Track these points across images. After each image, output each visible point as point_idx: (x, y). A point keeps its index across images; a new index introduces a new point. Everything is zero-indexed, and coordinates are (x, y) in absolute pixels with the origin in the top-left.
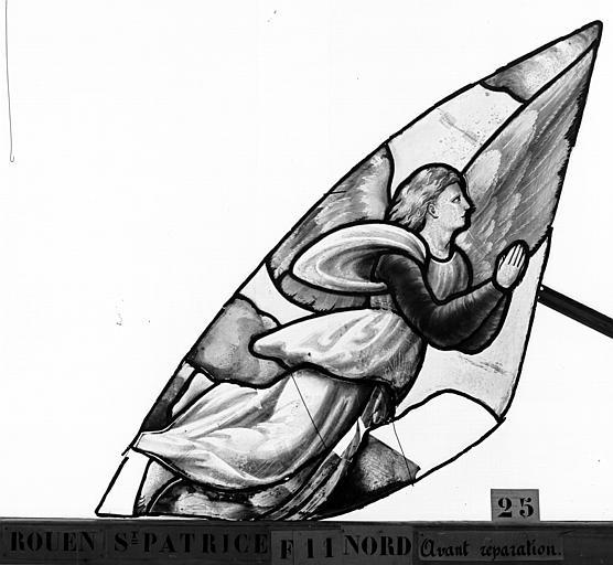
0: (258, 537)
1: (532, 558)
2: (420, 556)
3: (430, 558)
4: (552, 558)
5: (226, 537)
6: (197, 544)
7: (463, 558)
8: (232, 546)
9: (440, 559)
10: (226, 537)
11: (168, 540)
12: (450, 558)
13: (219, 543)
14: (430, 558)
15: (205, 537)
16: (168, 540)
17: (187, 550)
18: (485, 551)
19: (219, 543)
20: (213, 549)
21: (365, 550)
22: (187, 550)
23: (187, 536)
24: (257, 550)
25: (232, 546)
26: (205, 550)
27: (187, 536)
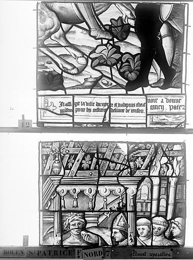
0: (69, 251)
1: (164, 257)
2: (133, 257)
3: (135, 257)
4: (169, 257)
5: (61, 251)
6: (52, 253)
7: (144, 257)
8: (62, 253)
9: (137, 257)
10: (61, 251)
11: (44, 252)
12: (141, 257)
13: (59, 253)
14: (135, 257)
15: (55, 251)
16: (44, 252)
17: (50, 255)
18: (151, 255)
19: (59, 253)
20: (57, 254)
21: (90, 256)
22: (50, 255)
23: (50, 251)
24: (69, 255)
25: (62, 253)
26: (55, 255)
27: (50, 251)
